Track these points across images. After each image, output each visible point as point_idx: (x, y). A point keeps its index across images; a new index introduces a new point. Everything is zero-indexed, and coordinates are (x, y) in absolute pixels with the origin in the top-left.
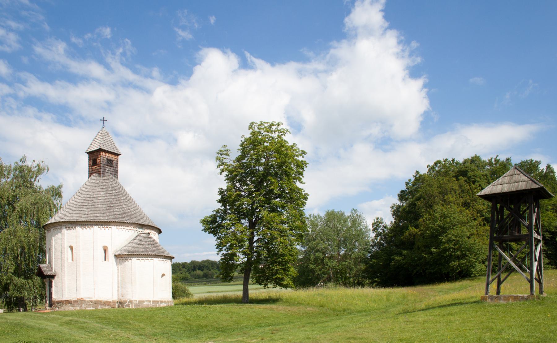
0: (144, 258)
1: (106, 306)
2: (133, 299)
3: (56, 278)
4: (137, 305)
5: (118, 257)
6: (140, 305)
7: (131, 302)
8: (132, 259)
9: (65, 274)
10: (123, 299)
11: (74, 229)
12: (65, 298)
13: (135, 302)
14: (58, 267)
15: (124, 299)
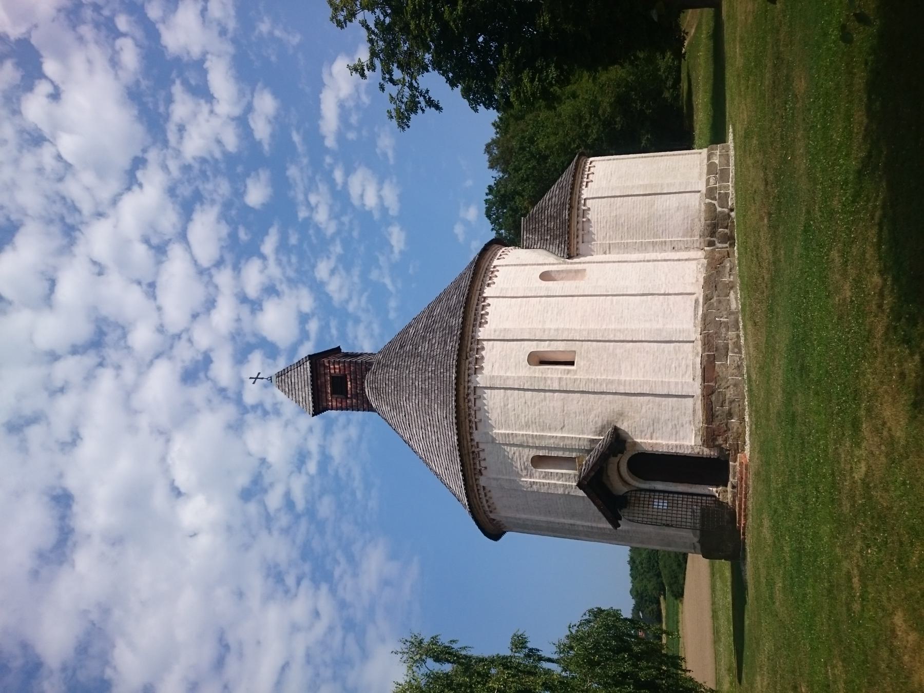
0: (586, 173)
1: (725, 267)
2: (703, 188)
3: (624, 426)
4: (721, 177)
5: (573, 250)
6: (721, 170)
7: (710, 193)
8: (584, 197)
9: (611, 382)
10: (700, 224)
11: (483, 348)
12: (696, 388)
13: (712, 181)
14: (590, 411)
15: (703, 215)
